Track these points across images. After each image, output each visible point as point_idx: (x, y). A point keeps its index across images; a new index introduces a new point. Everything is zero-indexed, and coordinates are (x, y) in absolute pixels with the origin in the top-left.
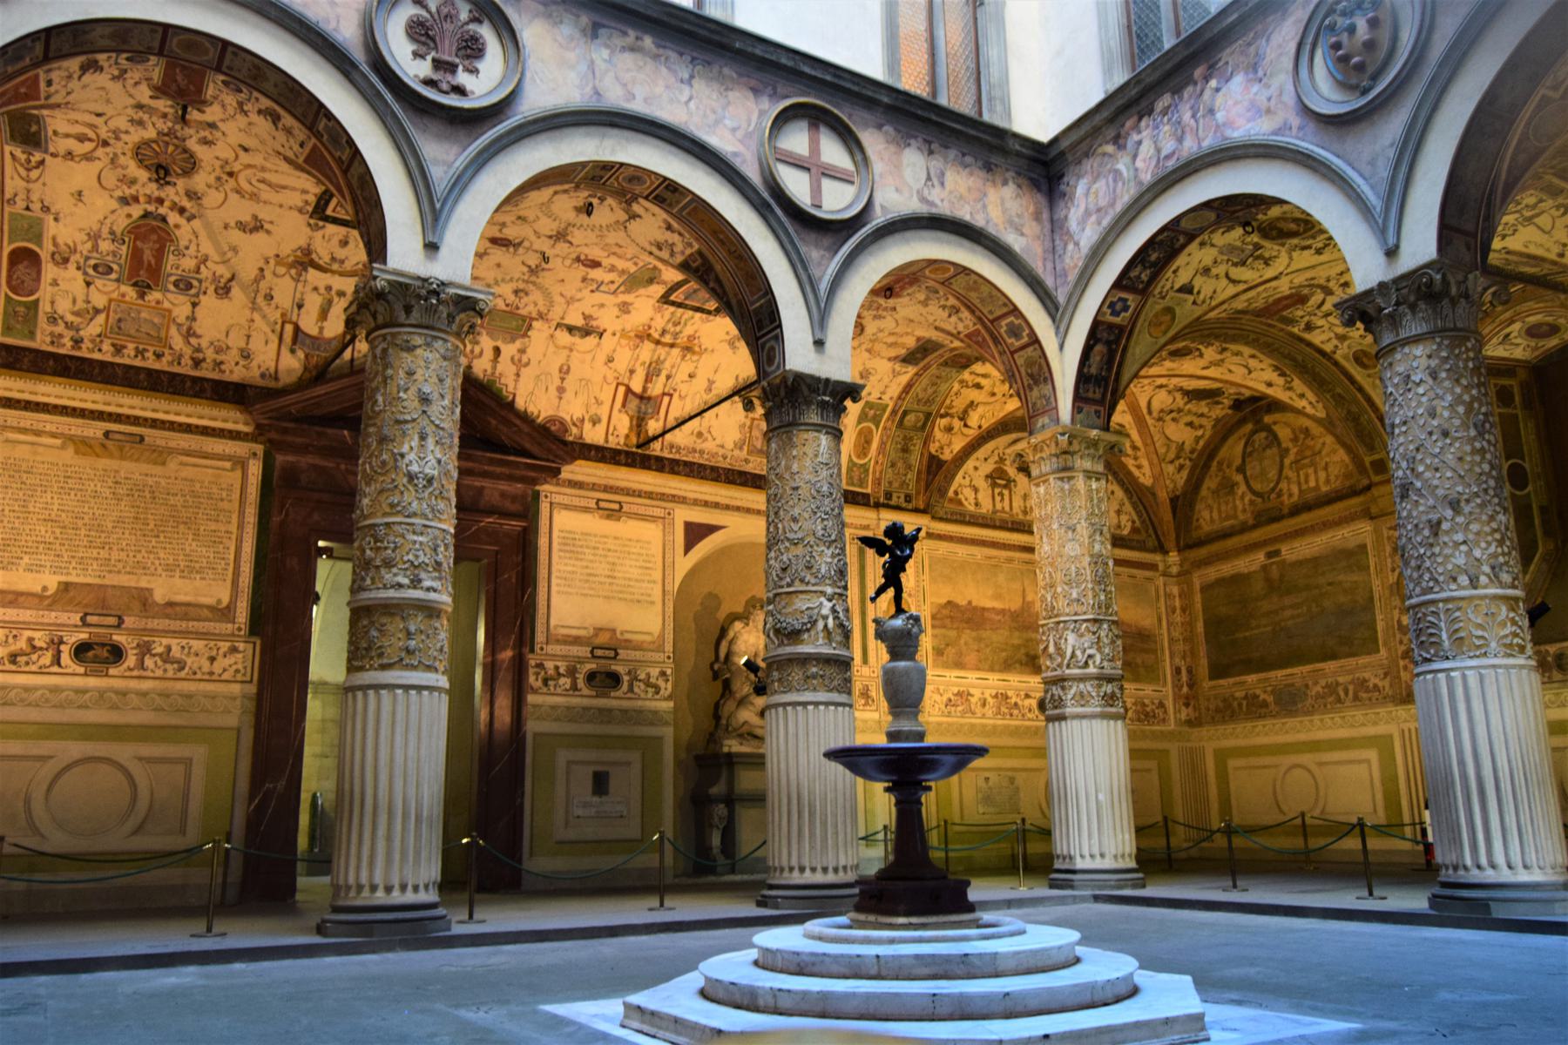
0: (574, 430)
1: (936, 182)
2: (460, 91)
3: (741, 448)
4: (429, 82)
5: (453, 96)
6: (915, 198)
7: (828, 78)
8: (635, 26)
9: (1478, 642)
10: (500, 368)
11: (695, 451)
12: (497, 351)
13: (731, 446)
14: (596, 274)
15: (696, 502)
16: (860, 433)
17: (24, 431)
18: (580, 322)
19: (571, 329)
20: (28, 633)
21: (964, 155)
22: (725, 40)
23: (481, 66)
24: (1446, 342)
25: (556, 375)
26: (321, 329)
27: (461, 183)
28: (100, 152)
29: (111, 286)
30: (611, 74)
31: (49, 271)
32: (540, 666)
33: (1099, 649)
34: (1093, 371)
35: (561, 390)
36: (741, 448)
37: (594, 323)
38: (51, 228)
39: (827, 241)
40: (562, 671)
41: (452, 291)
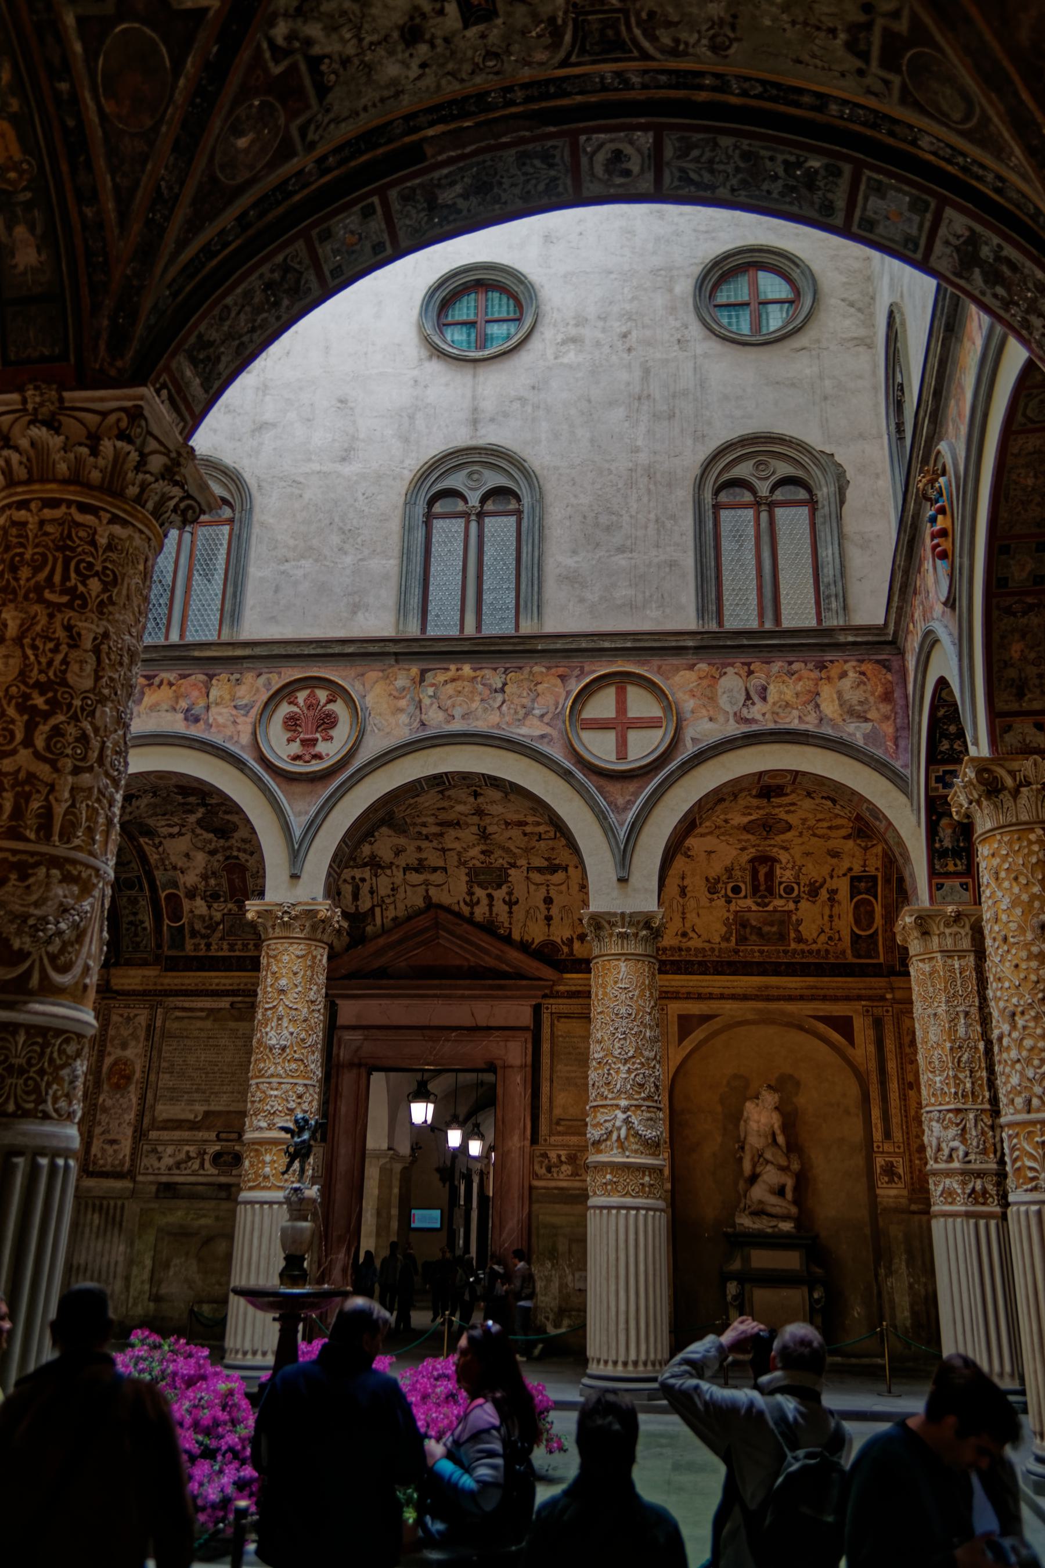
0: (566, 949)
1: (756, 698)
2: (318, 757)
3: (728, 940)
4: (297, 758)
5: (313, 762)
6: (732, 721)
7: (629, 645)
8: (453, 661)
9: (1031, 1174)
10: (495, 910)
11: (680, 949)
12: (490, 897)
13: (718, 939)
14: (528, 829)
15: (688, 997)
16: (857, 907)
17: (184, 1009)
18: (545, 864)
19: (540, 870)
20: (187, 1148)
21: (790, 663)
22: (528, 647)
23: (333, 733)
24: (1006, 839)
25: (542, 906)
26: (357, 907)
27: (313, 827)
28: (184, 830)
29: (223, 906)
30: (435, 706)
31: (186, 905)
32: (545, 1155)
33: (964, 1141)
34: (947, 843)
35: (549, 918)
36: (728, 940)
37: (557, 862)
38: (182, 879)
39: (632, 787)
40: (563, 1159)
41: (299, 908)
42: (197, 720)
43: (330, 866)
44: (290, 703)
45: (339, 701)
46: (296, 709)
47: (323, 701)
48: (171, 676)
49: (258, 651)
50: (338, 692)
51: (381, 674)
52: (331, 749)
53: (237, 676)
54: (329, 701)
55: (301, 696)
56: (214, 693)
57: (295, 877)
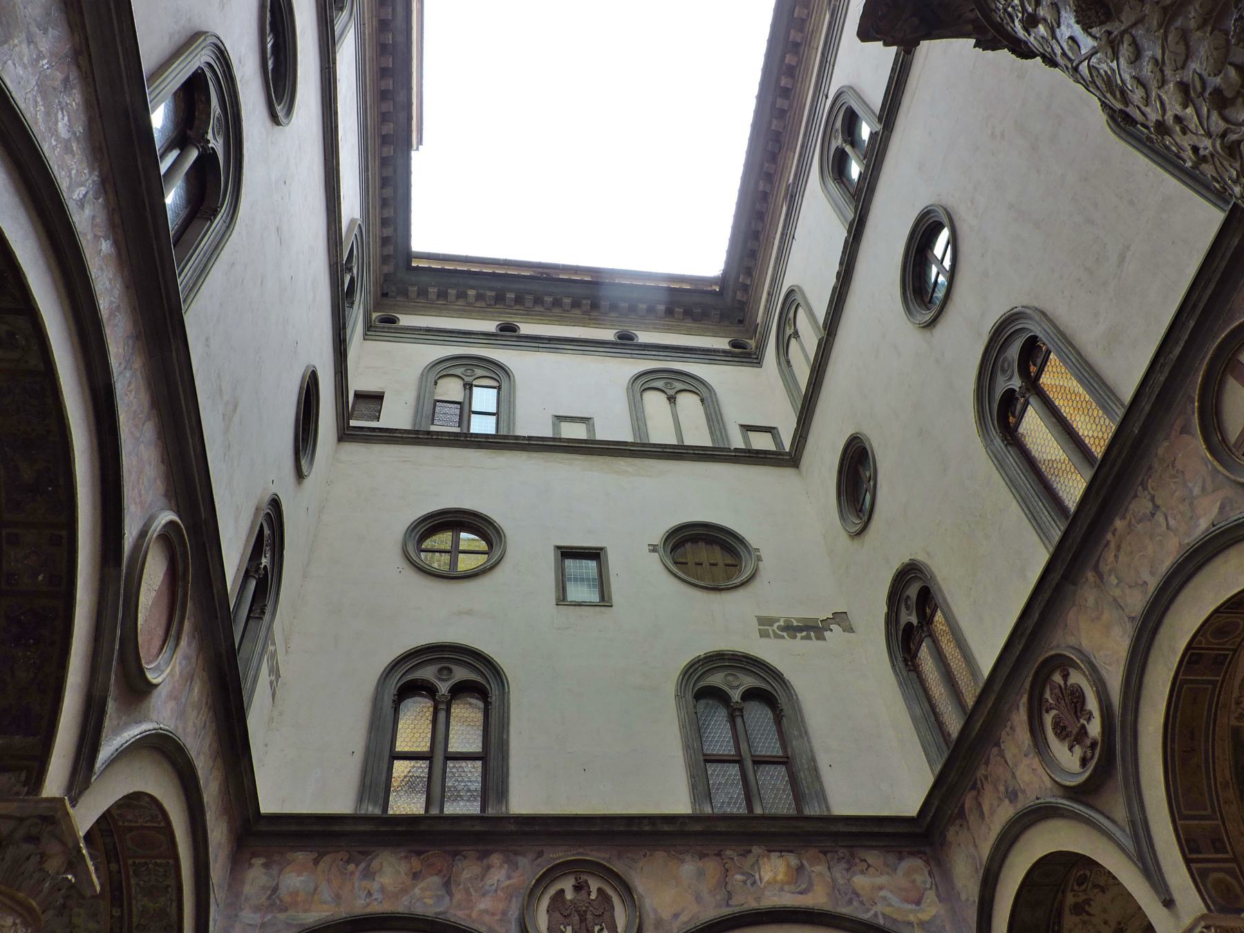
4: (1084, 762)
7: (1192, 323)
42: (1016, 795)
43: (1188, 862)
44: (1047, 712)
45: (1072, 672)
46: (1054, 712)
47: (1062, 683)
48: (981, 772)
49: (997, 687)
50: (1062, 663)
51: (1075, 608)
52: (1095, 729)
53: (1009, 724)
54: (1066, 677)
55: (1047, 695)
56: (1009, 756)
57: (1169, 903)
